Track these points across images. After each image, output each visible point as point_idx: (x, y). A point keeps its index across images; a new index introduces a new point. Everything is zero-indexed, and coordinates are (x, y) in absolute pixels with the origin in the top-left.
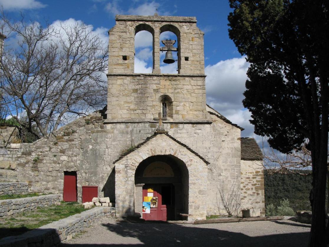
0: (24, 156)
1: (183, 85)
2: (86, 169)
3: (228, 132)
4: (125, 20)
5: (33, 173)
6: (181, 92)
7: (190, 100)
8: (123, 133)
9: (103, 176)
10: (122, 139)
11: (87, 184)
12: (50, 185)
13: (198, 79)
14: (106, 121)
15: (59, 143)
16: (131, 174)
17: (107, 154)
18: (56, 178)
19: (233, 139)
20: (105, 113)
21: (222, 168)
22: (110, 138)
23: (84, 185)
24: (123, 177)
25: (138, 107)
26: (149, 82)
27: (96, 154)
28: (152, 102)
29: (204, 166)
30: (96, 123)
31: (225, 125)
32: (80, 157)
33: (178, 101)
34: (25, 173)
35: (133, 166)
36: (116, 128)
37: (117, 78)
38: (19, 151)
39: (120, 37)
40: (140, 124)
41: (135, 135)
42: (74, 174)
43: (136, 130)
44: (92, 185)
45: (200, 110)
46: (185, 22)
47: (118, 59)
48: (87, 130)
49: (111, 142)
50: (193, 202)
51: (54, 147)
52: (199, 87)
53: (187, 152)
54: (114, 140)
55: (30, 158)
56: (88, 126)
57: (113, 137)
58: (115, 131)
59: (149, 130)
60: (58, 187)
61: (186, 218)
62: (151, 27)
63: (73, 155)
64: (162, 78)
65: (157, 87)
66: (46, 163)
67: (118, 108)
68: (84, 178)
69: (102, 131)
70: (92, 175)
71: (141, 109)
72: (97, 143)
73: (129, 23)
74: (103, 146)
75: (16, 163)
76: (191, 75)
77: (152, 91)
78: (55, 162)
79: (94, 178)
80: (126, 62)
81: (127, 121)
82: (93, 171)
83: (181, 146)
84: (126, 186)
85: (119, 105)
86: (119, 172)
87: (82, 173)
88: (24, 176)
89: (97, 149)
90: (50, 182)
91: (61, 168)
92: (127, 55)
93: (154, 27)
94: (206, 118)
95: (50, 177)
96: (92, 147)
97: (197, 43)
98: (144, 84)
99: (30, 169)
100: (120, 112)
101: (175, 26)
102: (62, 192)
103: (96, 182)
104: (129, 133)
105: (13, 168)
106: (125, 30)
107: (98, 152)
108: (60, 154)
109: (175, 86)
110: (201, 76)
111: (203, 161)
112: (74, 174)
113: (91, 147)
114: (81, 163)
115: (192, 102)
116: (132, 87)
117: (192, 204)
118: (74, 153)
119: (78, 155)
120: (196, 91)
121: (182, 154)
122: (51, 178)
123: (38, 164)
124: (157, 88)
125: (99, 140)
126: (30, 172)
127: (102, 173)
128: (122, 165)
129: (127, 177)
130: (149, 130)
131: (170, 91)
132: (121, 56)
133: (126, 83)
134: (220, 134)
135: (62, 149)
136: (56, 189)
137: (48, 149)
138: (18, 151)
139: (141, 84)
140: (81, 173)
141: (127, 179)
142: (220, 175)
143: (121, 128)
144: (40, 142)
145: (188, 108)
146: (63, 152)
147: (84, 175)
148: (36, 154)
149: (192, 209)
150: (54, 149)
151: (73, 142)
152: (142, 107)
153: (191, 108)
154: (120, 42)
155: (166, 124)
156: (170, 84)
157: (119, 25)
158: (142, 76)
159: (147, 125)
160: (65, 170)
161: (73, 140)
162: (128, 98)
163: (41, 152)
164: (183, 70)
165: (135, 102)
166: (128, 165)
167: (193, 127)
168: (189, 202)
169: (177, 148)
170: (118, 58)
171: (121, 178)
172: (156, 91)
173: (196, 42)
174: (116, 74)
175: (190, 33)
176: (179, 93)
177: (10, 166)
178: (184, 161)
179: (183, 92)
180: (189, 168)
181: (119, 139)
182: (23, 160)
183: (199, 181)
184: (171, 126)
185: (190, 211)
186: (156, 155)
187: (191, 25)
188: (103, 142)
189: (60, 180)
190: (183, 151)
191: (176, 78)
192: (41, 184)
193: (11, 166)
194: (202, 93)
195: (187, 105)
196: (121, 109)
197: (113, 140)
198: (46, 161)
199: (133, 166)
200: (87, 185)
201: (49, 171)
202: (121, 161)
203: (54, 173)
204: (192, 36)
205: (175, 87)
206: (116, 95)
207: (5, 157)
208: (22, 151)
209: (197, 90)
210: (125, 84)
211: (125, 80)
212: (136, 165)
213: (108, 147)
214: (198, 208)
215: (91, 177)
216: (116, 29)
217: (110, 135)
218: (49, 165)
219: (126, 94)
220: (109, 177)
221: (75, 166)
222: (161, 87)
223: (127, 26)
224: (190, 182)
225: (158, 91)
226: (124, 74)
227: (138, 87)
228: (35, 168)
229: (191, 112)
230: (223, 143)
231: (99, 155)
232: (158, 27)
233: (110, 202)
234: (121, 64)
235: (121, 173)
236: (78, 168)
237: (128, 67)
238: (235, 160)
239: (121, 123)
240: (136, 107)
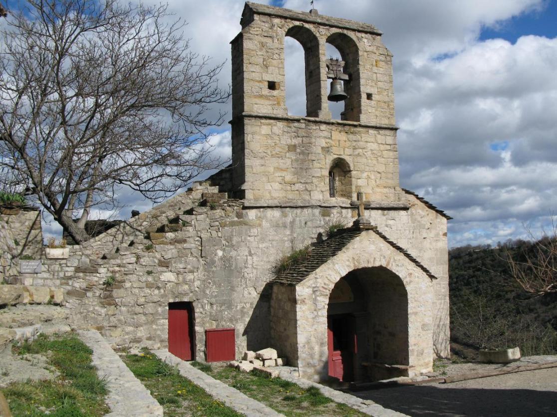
0: (81, 274)
1: (366, 142)
3: (431, 224)
4: (270, 15)
5: (103, 311)
6: (364, 154)
7: (376, 169)
8: (277, 226)
9: (243, 307)
10: (277, 238)
11: (214, 325)
12: (142, 333)
13: (388, 132)
15: (157, 246)
16: (323, 304)
17: (250, 266)
18: (153, 319)
19: (437, 235)
20: (242, 188)
22: (256, 236)
23: (208, 327)
24: (309, 310)
25: (298, 179)
26: (314, 134)
27: (230, 266)
28: (319, 169)
30: (228, 208)
31: (428, 213)
32: (200, 274)
33: (359, 169)
34: (85, 311)
35: (326, 289)
36: (265, 216)
37: (261, 123)
38: (69, 265)
39: (263, 45)
40: (305, 210)
41: (298, 230)
42: (188, 307)
44: (223, 326)
45: (391, 186)
46: (366, 32)
48: (212, 221)
49: (258, 243)
50: (415, 345)
51: (146, 254)
52: (389, 146)
53: (405, 261)
54: (262, 240)
55: (96, 279)
56: (214, 214)
57: (261, 234)
58: (264, 223)
59: (320, 221)
60: (159, 336)
61: (404, 373)
62: (313, 33)
63: (186, 270)
64: (334, 128)
65: (326, 143)
66: (132, 287)
67: (263, 179)
68: (208, 313)
69: (240, 223)
70: (223, 308)
71: (303, 181)
72: (233, 246)
73: (277, 21)
74: (244, 252)
75: (62, 290)
76: (378, 125)
77: (319, 150)
78: (149, 286)
79: (226, 313)
80: (275, 93)
81: (285, 205)
82: (225, 300)
83: (396, 250)
84: (314, 327)
85: (266, 174)
86: (303, 301)
87: (205, 304)
88: (85, 317)
89: (231, 257)
90: (142, 326)
91: (162, 298)
92: (275, 81)
93: (318, 35)
96: (223, 254)
97: (384, 71)
98: (306, 137)
99: (96, 301)
100: (268, 187)
101: (350, 36)
102: (167, 344)
103: (231, 320)
104: (288, 227)
105: (58, 301)
106: (270, 34)
107: (234, 263)
108: (160, 269)
109: (354, 144)
110: (392, 129)
111: (427, 274)
112: (188, 307)
113: (220, 253)
114: (203, 286)
115: (379, 173)
116: (287, 140)
117: (413, 347)
118: (189, 267)
119: (195, 270)
121: (398, 265)
123: (115, 290)
124: (327, 146)
125: (235, 240)
126: (96, 308)
127: (241, 302)
129: (315, 310)
130: (320, 221)
131: (348, 151)
134: (421, 226)
135: (162, 259)
136: (154, 340)
137: (134, 260)
138: (66, 264)
139: (302, 137)
140: (202, 305)
141: (315, 313)
143: (274, 217)
144: (99, 243)
145: (374, 182)
146: (165, 264)
147: (208, 307)
148: (108, 270)
150: (147, 259)
151: (185, 245)
152: (305, 179)
153: (378, 182)
154: (262, 55)
155: (346, 210)
156: (346, 139)
157: (259, 22)
158: (302, 121)
159: (317, 211)
160: (171, 301)
161: (185, 241)
162: (281, 161)
163: (119, 266)
164: (364, 116)
165: (293, 170)
166: (318, 287)
167: (384, 215)
168: (409, 345)
169: (391, 254)
170: (261, 85)
171: (307, 313)
172: (327, 150)
174: (261, 115)
176: (361, 156)
177: (52, 297)
178: (401, 276)
179: (365, 153)
181: (271, 238)
182: (79, 284)
183: (422, 308)
184: (352, 214)
185: (412, 360)
186: (360, 267)
187: (374, 39)
188: (242, 244)
189: (162, 321)
190: (399, 260)
191: (355, 129)
192: (123, 331)
193: (55, 297)
194: (393, 157)
195: (373, 177)
196: (269, 182)
197: (261, 240)
198: (130, 284)
199: (326, 289)
200: (214, 327)
201: (137, 305)
202: (306, 281)
203: (150, 309)
204: (376, 57)
205: (354, 145)
206: (260, 155)
207: (37, 278)
208: (75, 265)
209: (386, 152)
210: (274, 134)
211: (275, 128)
213: (253, 252)
214: (422, 354)
215: (221, 311)
216: (255, 29)
217: (254, 231)
218: (137, 291)
219: (277, 154)
220: (255, 309)
221: (192, 292)
222: (333, 143)
223: (274, 25)
224: (410, 311)
225: (328, 151)
226: (274, 116)
228: (108, 300)
231: (236, 268)
232: (324, 35)
233: (279, 357)
234: (267, 95)
235: (306, 304)
236: (197, 296)
237: (278, 104)
238: (441, 269)
239: (274, 209)
240: (294, 178)
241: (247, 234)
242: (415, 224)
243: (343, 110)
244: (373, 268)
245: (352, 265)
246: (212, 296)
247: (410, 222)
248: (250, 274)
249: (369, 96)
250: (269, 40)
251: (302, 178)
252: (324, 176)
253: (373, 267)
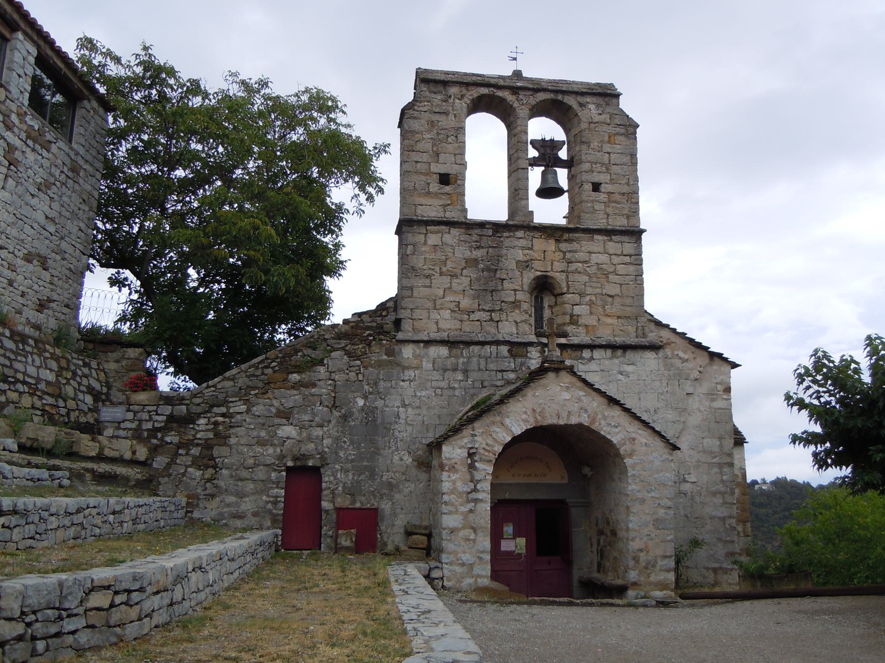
0: (175, 425)
1: (590, 253)
14: (400, 336)
17: (403, 422)
27: (374, 420)
29: (665, 456)
32: (332, 429)
35: (489, 452)
38: (159, 412)
39: (432, 124)
40: (487, 347)
42: (316, 472)
47: (429, 181)
58: (424, 363)
63: (313, 424)
66: (238, 444)
70: (363, 477)
77: (513, 265)
80: (447, 189)
87: (337, 471)
89: (376, 408)
92: (450, 172)
93: (516, 105)
94: (644, 335)
95: (247, 482)
100: (435, 315)
108: (277, 421)
113: (361, 402)
116: (463, 252)
119: (326, 424)
120: (621, 269)
122: (251, 486)
124: (525, 259)
128: (460, 449)
135: (281, 408)
138: (156, 411)
144: (213, 389)
146: (286, 415)
151: (313, 390)
161: (314, 385)
163: (223, 415)
165: (472, 292)
166: (476, 449)
172: (525, 265)
173: (618, 147)
175: (604, 123)
179: (588, 269)
180: (628, 461)
188: (393, 390)
190: (613, 416)
193: (138, 453)
199: (489, 452)
203: (261, 473)
204: (610, 129)
208: (168, 413)
212: (496, 449)
222: (536, 255)
223: (450, 96)
225: (527, 266)
227: (478, 254)
230: (690, 400)
235: (456, 471)
241: (398, 378)
242: (671, 373)
243: (566, 211)
244: (567, 427)
245: (532, 420)
247: (662, 369)
248: (403, 432)
249: (596, 187)
250: (442, 118)
253: (566, 425)
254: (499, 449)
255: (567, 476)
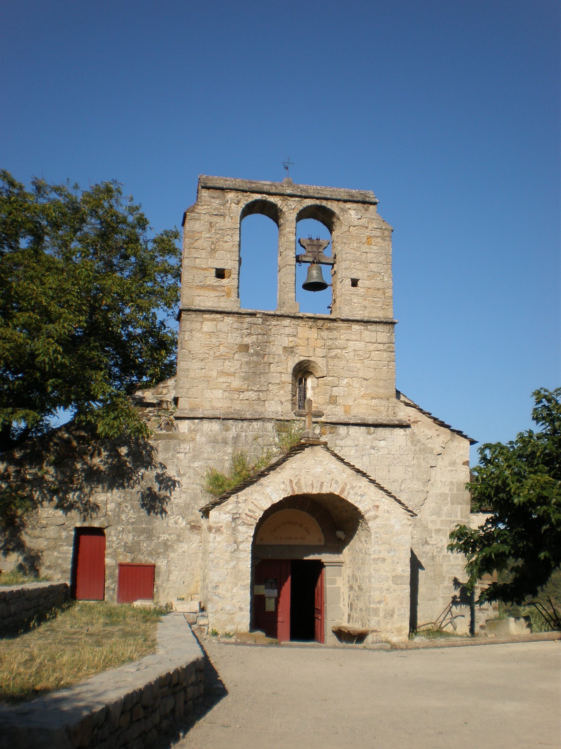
1: (348, 340)
2: (128, 523)
7: (361, 375)
11: (127, 559)
13: (380, 327)
16: (246, 535)
19: (453, 463)
21: (431, 526)
22: (186, 453)
31: (438, 432)
35: (251, 517)
40: (255, 423)
43: (246, 436)
45: (383, 396)
47: (207, 275)
57: (194, 450)
58: (198, 437)
70: (142, 538)
73: (231, 195)
77: (280, 351)
80: (224, 281)
81: (226, 417)
82: (144, 528)
85: (207, 380)
100: (208, 394)
109: (330, 343)
116: (235, 339)
124: (291, 345)
128: (225, 514)
132: (213, 268)
133: (225, 329)
134: (425, 450)
142: (427, 543)
143: (211, 431)
149: (378, 616)
154: (210, 238)
160: (78, 525)
165: (243, 374)
166: (240, 514)
167: (369, 433)
172: (290, 350)
173: (375, 248)
174: (202, 309)
175: (363, 226)
191: (332, 324)
199: (251, 517)
204: (368, 233)
209: (377, 352)
212: (257, 514)
213: (182, 472)
214: (392, 616)
217: (186, 447)
223: (228, 201)
225: (292, 352)
226: (220, 309)
227: (248, 340)
229: (365, 401)
234: (213, 286)
236: (109, 521)
241: (175, 450)
242: (417, 448)
244: (319, 495)
246: (128, 523)
247: (410, 445)
249: (354, 283)
251: (255, 384)
252: (283, 383)
253: (319, 494)
254: (259, 514)
255: (323, 539)
